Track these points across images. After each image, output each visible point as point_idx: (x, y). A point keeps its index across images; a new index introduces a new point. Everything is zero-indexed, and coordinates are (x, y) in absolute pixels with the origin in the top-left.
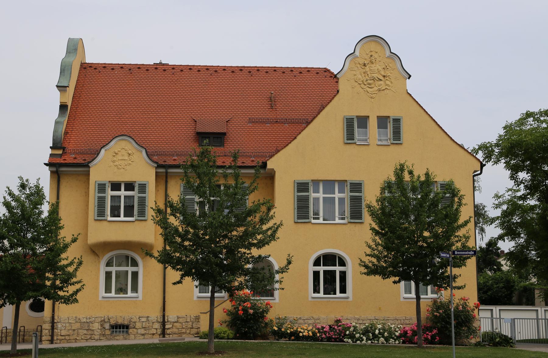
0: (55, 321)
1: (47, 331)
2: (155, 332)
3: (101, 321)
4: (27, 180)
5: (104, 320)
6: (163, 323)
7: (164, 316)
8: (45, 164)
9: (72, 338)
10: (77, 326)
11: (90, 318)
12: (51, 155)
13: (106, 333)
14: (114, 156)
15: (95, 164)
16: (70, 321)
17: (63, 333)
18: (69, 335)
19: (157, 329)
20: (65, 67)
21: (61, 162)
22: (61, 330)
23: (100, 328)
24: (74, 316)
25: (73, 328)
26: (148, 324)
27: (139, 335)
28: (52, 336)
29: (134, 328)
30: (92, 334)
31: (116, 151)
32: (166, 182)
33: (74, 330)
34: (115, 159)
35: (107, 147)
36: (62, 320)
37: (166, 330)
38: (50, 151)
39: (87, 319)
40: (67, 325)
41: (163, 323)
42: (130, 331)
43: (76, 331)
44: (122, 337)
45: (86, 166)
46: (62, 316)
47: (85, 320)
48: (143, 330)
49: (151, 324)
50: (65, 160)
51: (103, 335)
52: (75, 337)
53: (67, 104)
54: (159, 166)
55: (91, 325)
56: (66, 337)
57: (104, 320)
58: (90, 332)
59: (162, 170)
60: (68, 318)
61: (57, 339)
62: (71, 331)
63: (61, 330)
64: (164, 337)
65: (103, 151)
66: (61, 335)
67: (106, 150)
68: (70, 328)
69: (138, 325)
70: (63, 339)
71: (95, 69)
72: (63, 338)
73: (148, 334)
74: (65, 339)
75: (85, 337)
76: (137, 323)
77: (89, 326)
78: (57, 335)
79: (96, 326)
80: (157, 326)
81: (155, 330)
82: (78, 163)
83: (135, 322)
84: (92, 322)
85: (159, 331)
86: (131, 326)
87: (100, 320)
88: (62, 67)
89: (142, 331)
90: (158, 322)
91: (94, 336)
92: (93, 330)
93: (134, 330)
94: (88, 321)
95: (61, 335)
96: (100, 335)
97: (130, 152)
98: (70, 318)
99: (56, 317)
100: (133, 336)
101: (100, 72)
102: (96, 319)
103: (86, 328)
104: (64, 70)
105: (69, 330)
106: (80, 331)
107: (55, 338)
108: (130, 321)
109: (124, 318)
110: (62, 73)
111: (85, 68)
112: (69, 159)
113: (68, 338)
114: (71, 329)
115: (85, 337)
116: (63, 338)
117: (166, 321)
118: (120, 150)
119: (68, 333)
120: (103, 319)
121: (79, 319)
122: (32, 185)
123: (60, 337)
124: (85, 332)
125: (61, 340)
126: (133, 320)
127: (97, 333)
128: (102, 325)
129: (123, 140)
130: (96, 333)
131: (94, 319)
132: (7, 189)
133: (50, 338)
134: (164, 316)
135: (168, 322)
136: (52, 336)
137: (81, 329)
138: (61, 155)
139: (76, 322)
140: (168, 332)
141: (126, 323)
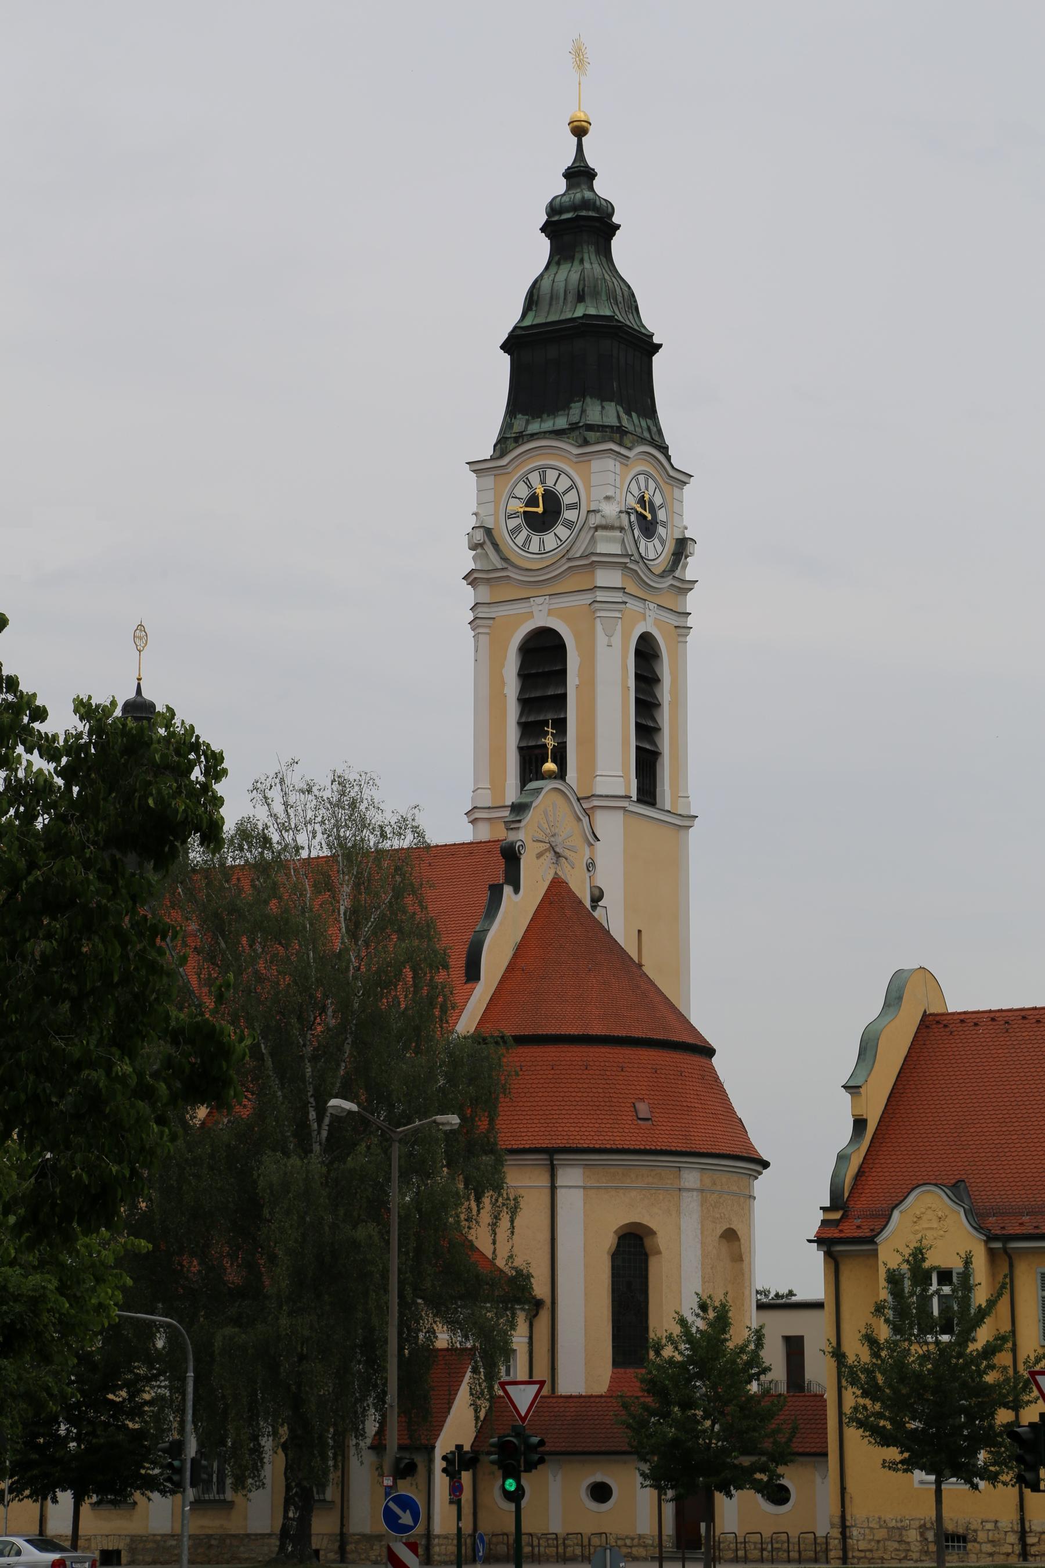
0: (848, 1524)
1: (836, 1541)
2: (1010, 1551)
3: (920, 1527)
4: (710, 1297)
5: (924, 1525)
6: (1023, 1534)
7: (1022, 1520)
8: (810, 1241)
9: (876, 1555)
10: (881, 1534)
11: (901, 1521)
12: (824, 1222)
13: (930, 1550)
14: (915, 1222)
15: (886, 1239)
16: (871, 1525)
17: (862, 1545)
18: (871, 1551)
19: (1013, 1545)
20: (867, 1044)
21: (835, 1235)
22: (858, 1541)
23: (919, 1539)
24: (877, 1516)
25: (876, 1538)
26: (997, 1535)
27: (984, 1555)
28: (845, 1550)
29: (975, 1541)
30: (908, 1550)
31: (918, 1213)
32: (1011, 1266)
33: (878, 1542)
34: (917, 1228)
35: (902, 1207)
36: (857, 1522)
37: (1028, 1548)
38: (820, 1216)
39: (896, 1521)
40: (867, 1531)
41: (1023, 1534)
42: (969, 1546)
43: (881, 1544)
44: (956, 1557)
45: (871, 1240)
46: (858, 1516)
47: (893, 1524)
48: (989, 1545)
49: (1002, 1535)
50: (841, 1231)
51: (926, 1552)
52: (880, 1554)
53: (865, 1117)
54: (990, 1238)
55: (904, 1533)
56: (867, 1553)
57: (924, 1525)
58: (903, 1547)
59: (998, 1245)
60: (868, 1519)
61: (853, 1557)
62: (873, 1544)
63: (858, 1541)
64: (1025, 1559)
65: (896, 1214)
66: (858, 1550)
67: (901, 1212)
68: (871, 1537)
69: (982, 1536)
70: (862, 1558)
71: (946, 1026)
72: (862, 1554)
73: (999, 1553)
74: (865, 1557)
75: (897, 1555)
76: (979, 1533)
77: (901, 1535)
78: (853, 1550)
79: (913, 1535)
80: (1013, 1538)
81: (1011, 1546)
82: (860, 1237)
83: (975, 1531)
84: (904, 1528)
85: (1018, 1549)
86: (970, 1536)
87: (917, 1524)
88: (863, 1044)
89: (988, 1548)
90: (1013, 1531)
91: (910, 1553)
92: (908, 1543)
93: (975, 1544)
94: (899, 1525)
95: (858, 1550)
96: (921, 1551)
97: (940, 1214)
98: (871, 1519)
99: (848, 1517)
100: (974, 1556)
101: (951, 1032)
102: (912, 1522)
103: (897, 1538)
104: (865, 1049)
105: (870, 1541)
106: (888, 1543)
107: (850, 1555)
108: (967, 1529)
109: (957, 1522)
110: (862, 1057)
111: (927, 1027)
112: (849, 1230)
113: (871, 1556)
114: (873, 1540)
115: (897, 1555)
116: (862, 1554)
117: (1028, 1530)
118: (923, 1210)
119: (869, 1547)
120: (922, 1522)
121: (885, 1522)
122: (717, 1304)
123: (856, 1554)
124: (896, 1545)
125: (859, 1559)
126: (972, 1527)
127: (916, 1547)
128: (922, 1534)
129: (928, 1191)
130: (913, 1547)
131: (908, 1521)
132: (676, 1315)
133: (840, 1554)
134: (1022, 1520)
135: (1031, 1532)
136: (845, 1550)
137: (889, 1540)
138: (836, 1223)
139: (881, 1527)
140: (1033, 1550)
141: (961, 1531)
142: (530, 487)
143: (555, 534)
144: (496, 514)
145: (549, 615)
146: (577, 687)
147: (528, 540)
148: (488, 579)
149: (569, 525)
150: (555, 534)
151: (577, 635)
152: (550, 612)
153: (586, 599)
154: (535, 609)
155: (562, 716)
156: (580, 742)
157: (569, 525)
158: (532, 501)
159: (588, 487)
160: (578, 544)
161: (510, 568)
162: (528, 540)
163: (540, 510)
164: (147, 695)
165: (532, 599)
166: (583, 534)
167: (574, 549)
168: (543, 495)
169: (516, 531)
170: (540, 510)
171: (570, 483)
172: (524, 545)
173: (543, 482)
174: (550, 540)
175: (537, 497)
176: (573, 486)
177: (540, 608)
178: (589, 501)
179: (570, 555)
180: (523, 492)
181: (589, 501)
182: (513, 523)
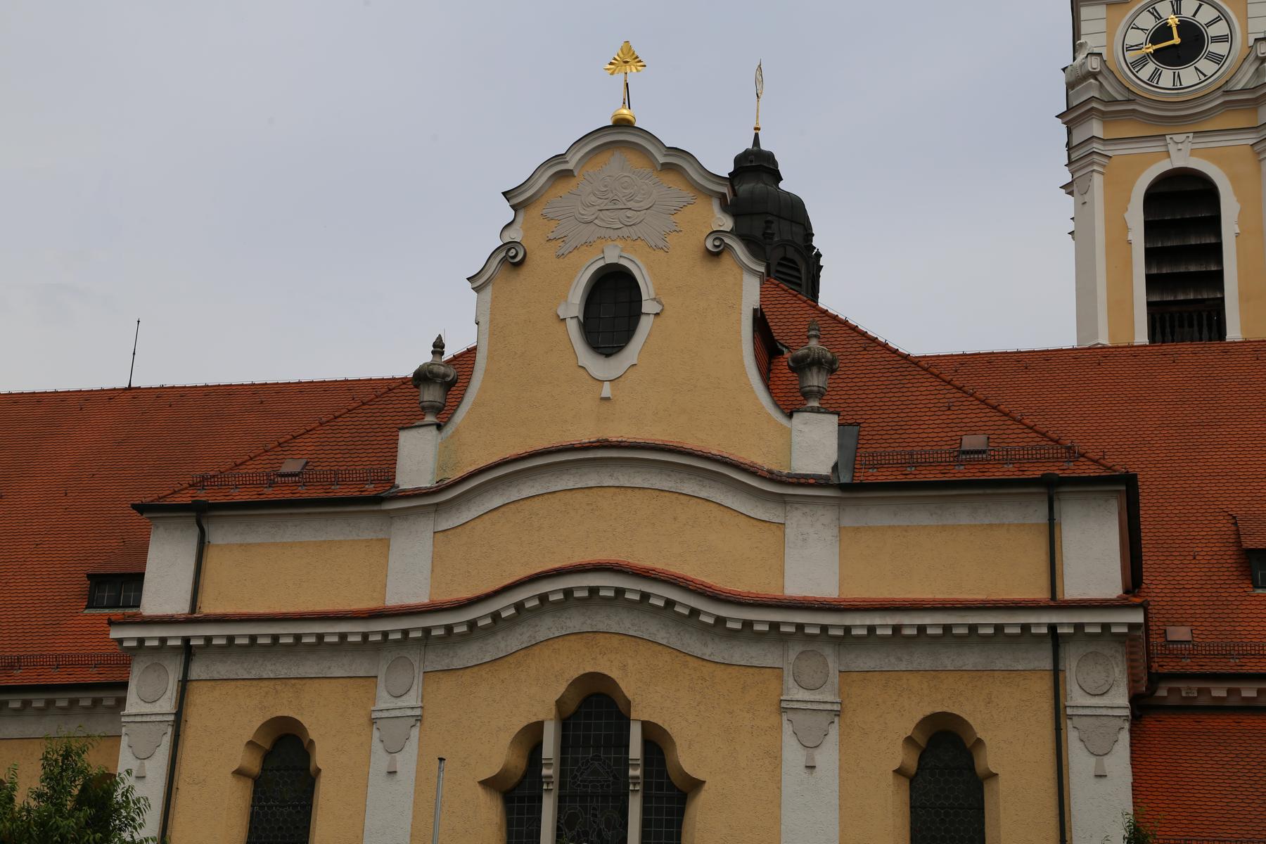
142: (1158, 17)
143: (1196, 68)
144: (1110, 45)
145: (1191, 155)
146: (1237, 235)
147: (1156, 74)
148: (1103, 113)
149: (1217, 59)
150: (1196, 68)
151: (1234, 179)
152: (1193, 152)
153: (1250, 139)
154: (1172, 148)
155: (1213, 268)
156: (1244, 297)
157: (1217, 59)
158: (1162, 32)
159: (1245, 19)
160: (1239, 76)
161: (1139, 100)
162: (1156, 74)
163: (1177, 40)
164: (764, 146)
165: (1168, 137)
166: (1246, 65)
167: (1234, 81)
168: (1178, 26)
169: (1142, 62)
170: (1177, 40)
171: (1216, 14)
172: (1151, 78)
173: (1177, 11)
174: (1188, 75)
175: (1170, 28)
176: (1222, 16)
177: (1180, 146)
178: (1246, 33)
179: (1229, 87)
180: (1148, 22)
181: (1246, 33)
182: (1132, 57)
